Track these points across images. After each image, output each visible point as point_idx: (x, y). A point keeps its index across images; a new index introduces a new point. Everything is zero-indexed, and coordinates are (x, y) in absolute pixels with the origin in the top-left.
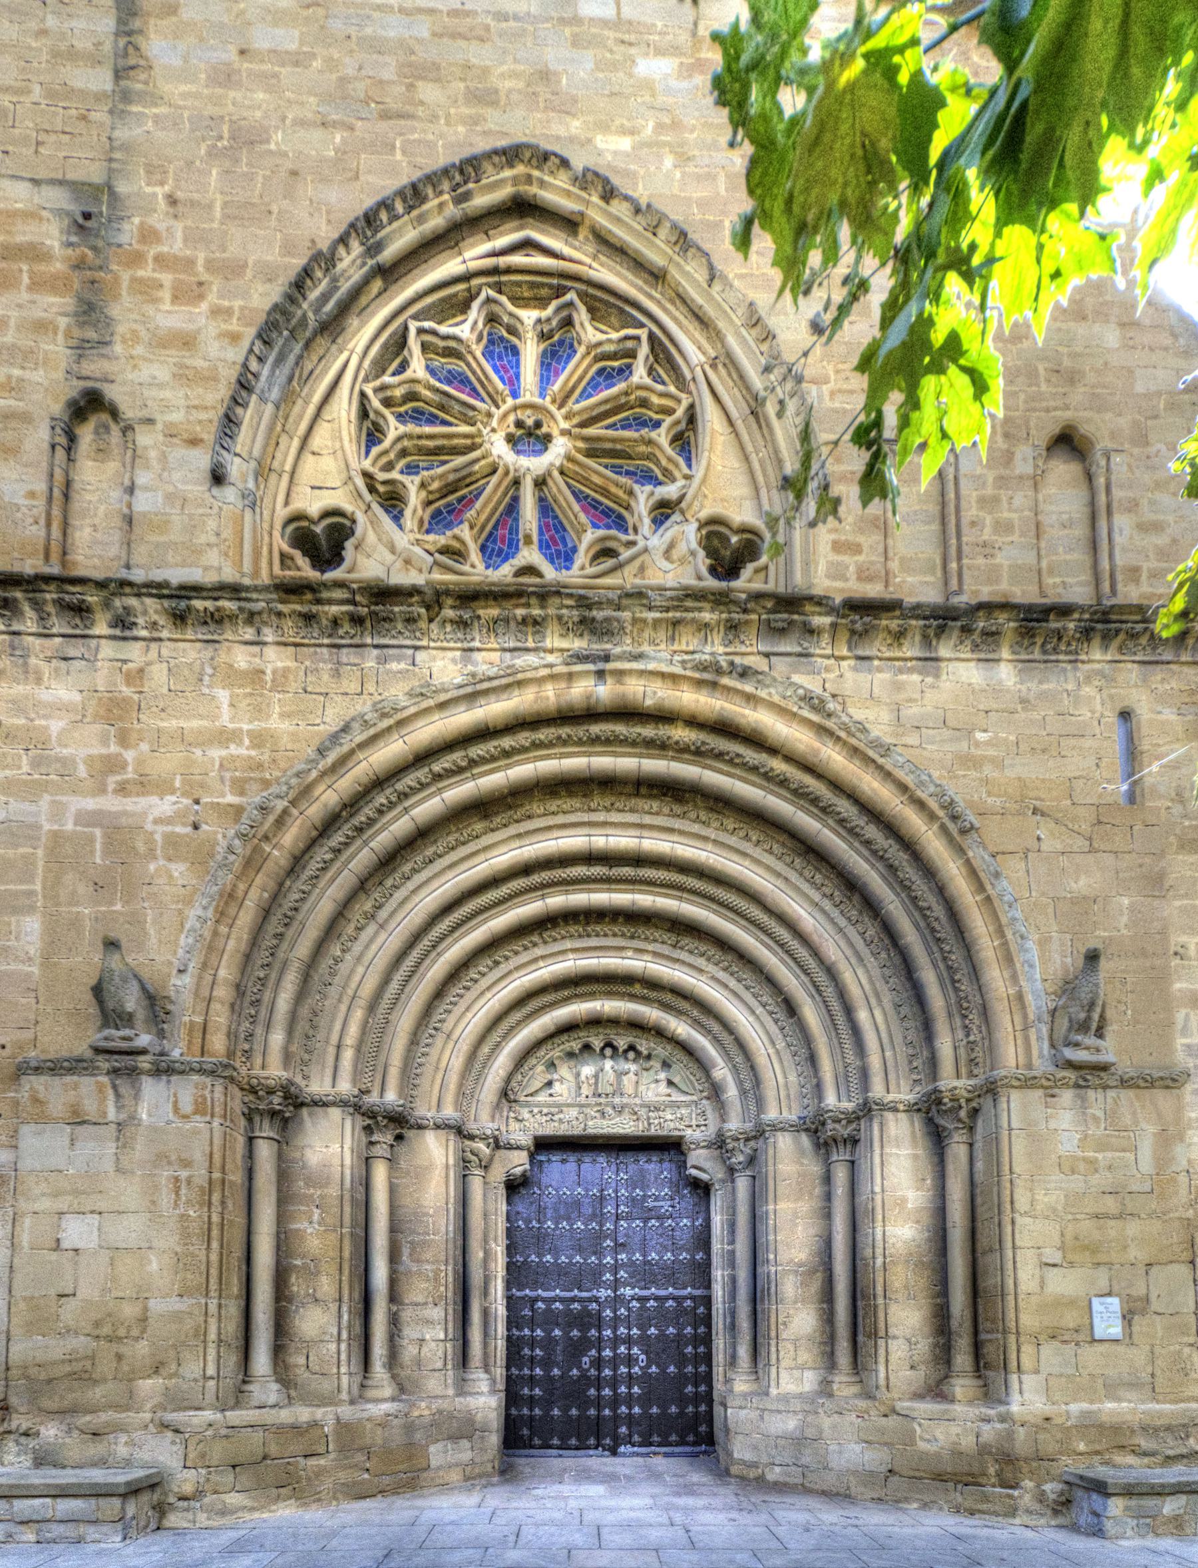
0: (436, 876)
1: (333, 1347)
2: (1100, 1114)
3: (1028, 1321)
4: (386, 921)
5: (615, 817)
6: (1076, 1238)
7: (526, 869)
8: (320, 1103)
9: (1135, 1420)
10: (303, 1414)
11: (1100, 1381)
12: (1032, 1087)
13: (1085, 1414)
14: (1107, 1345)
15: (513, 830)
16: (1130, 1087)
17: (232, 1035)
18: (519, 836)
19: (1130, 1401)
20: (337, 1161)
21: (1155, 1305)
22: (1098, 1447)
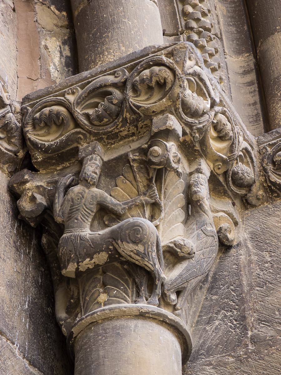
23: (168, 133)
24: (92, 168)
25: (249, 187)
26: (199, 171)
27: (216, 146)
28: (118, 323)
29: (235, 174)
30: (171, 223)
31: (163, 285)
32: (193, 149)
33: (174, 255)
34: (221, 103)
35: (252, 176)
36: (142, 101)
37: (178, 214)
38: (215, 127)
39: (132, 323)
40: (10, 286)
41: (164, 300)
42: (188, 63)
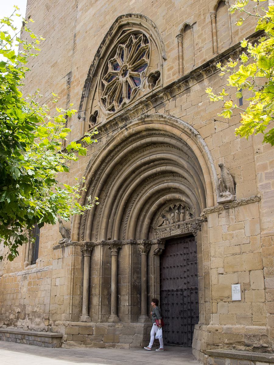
0: (116, 181)
1: (98, 307)
2: (233, 217)
3: (215, 294)
4: (109, 196)
5: (145, 153)
6: (228, 263)
7: (133, 172)
8: (97, 245)
9: (243, 332)
10: (91, 324)
11: (235, 316)
12: (214, 212)
13: (228, 329)
14: (237, 303)
15: (128, 165)
16: (241, 205)
17: (79, 234)
18: (129, 165)
19: (244, 324)
20: (100, 259)
21: (253, 287)
22: (231, 342)
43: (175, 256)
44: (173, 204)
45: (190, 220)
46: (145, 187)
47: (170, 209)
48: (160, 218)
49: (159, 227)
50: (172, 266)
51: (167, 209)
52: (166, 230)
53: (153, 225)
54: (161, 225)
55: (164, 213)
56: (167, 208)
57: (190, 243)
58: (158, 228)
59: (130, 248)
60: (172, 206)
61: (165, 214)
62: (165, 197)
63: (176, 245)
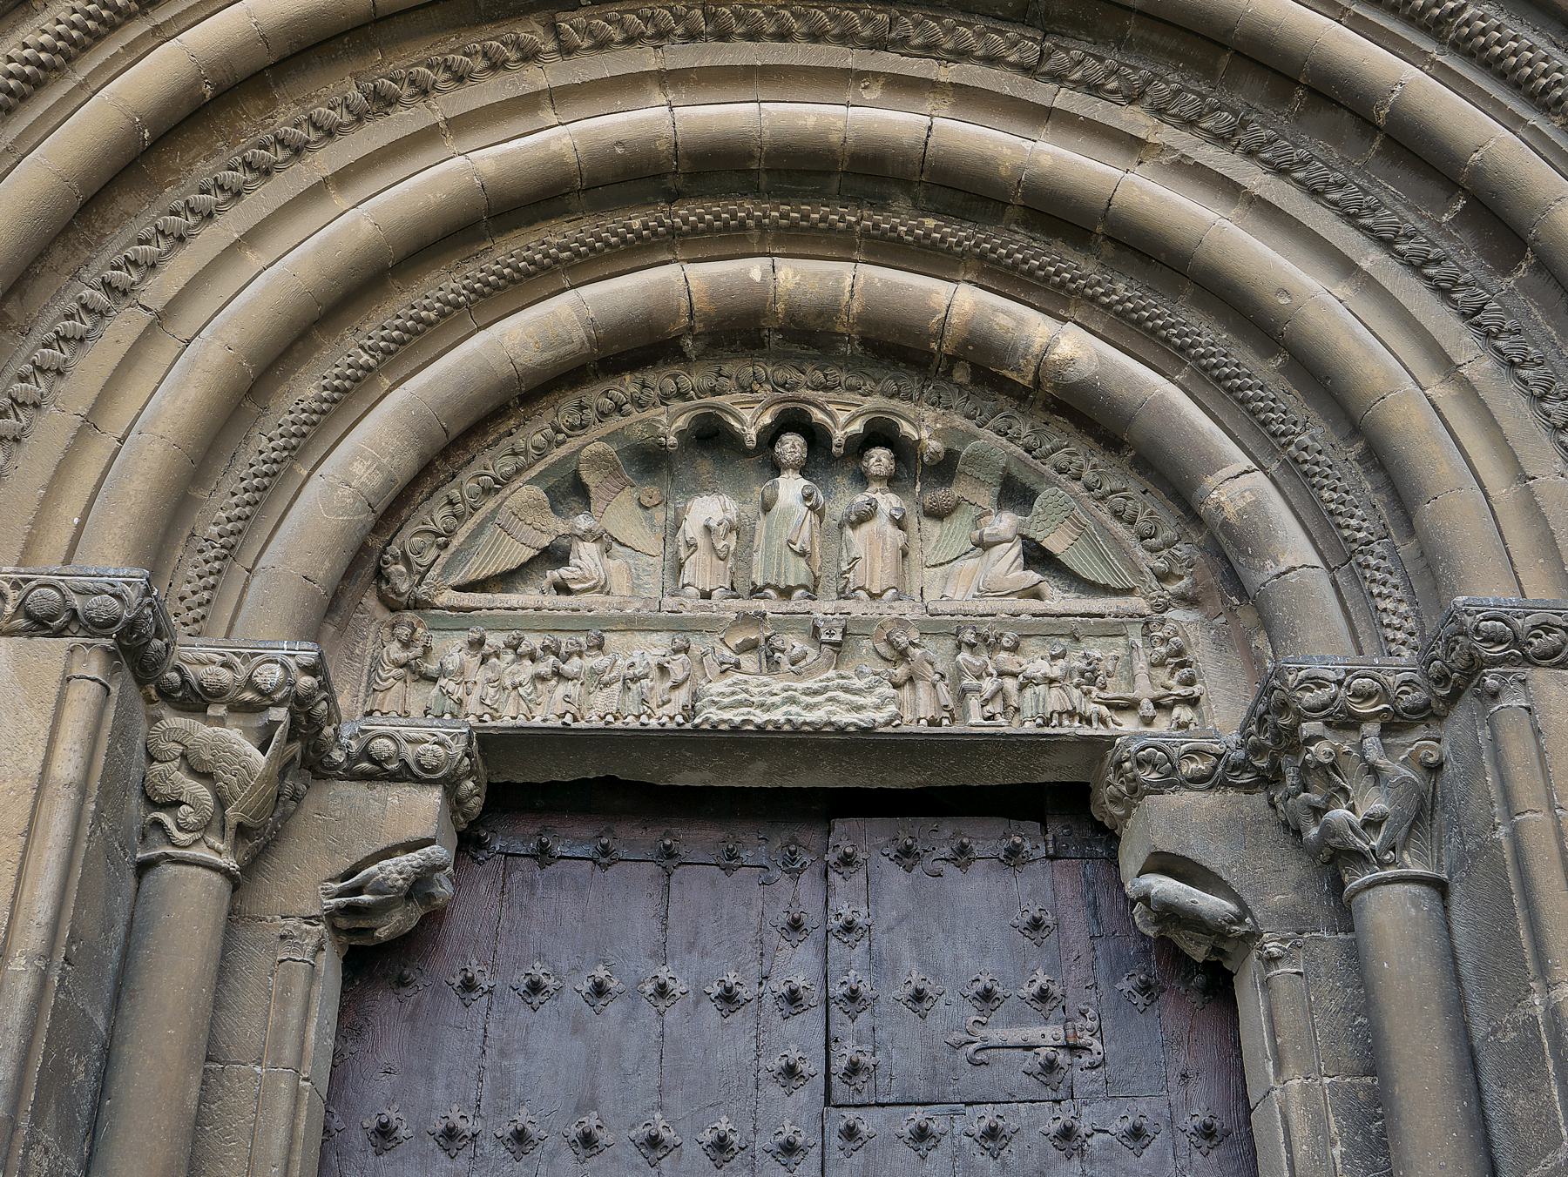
23: (1311, 740)
24: (1291, 781)
25: (1428, 705)
26: (1364, 737)
27: (1364, 709)
28: (1358, 898)
29: (1405, 710)
30: (1362, 794)
31: (1373, 851)
32: (1349, 723)
33: (1372, 824)
34: (1348, 672)
35: (1425, 696)
36: (1284, 721)
37: (1367, 780)
38: (1354, 695)
39: (1366, 895)
40: (1299, 887)
41: (1383, 865)
42: (1291, 678)
43: (614, 1009)
44: (765, 393)
45: (1035, 605)
46: (530, 56)
47: (711, 437)
48: (526, 493)
49: (468, 599)
50: (550, 1121)
51: (670, 423)
52: (600, 647)
53: (409, 538)
54: (506, 580)
55: (598, 461)
56: (659, 414)
57: (896, 879)
58: (448, 597)
59: (82, 698)
60: (750, 420)
61: (589, 478)
62: (755, 269)
63: (650, 869)
